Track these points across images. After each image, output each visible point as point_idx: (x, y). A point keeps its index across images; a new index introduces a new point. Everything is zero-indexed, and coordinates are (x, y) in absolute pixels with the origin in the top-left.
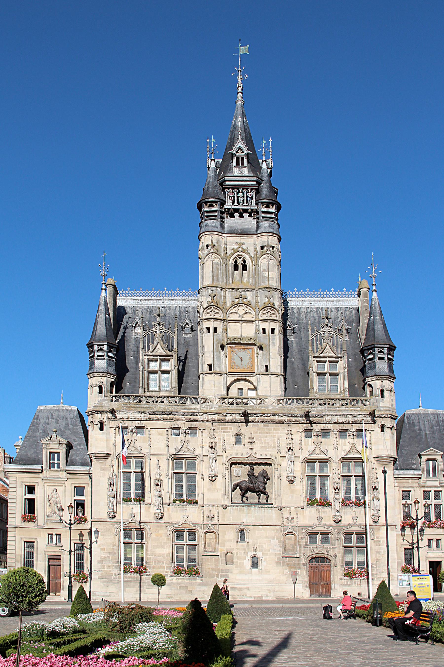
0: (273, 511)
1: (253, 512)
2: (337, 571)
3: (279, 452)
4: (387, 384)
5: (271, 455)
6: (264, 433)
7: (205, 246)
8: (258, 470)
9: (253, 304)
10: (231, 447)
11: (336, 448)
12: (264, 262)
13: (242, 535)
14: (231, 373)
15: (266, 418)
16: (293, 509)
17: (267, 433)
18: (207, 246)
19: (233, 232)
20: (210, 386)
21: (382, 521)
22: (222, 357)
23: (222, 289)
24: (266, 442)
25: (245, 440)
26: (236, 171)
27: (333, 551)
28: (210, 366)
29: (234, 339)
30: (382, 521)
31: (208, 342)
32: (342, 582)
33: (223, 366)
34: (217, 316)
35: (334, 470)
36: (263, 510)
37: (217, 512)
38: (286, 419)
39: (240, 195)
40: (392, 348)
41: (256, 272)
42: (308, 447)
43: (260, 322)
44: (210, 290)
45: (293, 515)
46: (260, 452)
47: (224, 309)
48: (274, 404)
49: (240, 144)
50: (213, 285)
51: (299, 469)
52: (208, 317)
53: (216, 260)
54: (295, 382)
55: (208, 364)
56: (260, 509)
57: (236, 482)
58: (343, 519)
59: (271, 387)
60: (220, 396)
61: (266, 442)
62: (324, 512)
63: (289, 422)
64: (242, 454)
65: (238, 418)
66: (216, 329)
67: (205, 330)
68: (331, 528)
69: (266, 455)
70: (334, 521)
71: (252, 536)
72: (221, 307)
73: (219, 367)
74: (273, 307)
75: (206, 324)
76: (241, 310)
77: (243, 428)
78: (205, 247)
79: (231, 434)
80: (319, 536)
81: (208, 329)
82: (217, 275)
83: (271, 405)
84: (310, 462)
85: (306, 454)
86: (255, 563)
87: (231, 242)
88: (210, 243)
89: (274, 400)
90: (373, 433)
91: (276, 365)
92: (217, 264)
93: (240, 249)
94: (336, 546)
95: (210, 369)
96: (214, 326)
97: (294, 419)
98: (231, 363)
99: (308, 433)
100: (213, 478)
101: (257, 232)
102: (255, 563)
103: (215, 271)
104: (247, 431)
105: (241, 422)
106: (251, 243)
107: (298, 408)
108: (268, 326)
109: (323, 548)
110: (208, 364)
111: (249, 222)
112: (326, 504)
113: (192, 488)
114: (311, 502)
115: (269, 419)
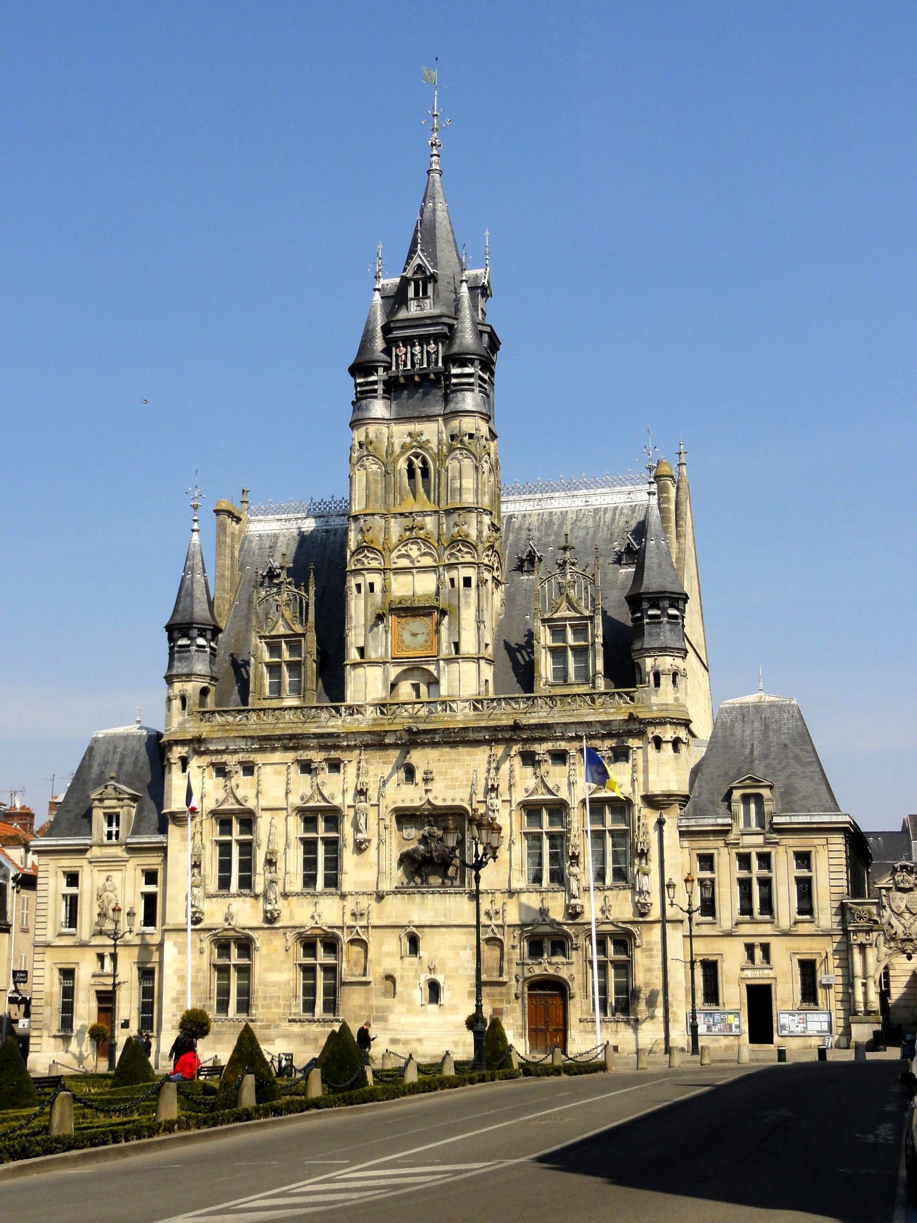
2: (575, 1007)
3: (473, 793)
5: (462, 800)
6: (450, 760)
7: (357, 445)
9: (434, 541)
10: (395, 790)
11: (572, 783)
14: (397, 661)
16: (498, 895)
17: (456, 760)
18: (361, 445)
21: (655, 913)
23: (383, 516)
25: (419, 776)
26: (413, 305)
27: (568, 969)
28: (362, 651)
29: (400, 603)
30: (655, 913)
31: (358, 609)
32: (585, 1028)
33: (381, 651)
34: (374, 564)
39: (418, 348)
44: (362, 521)
46: (446, 793)
47: (383, 552)
48: (467, 710)
50: (368, 511)
53: (375, 467)
55: (357, 648)
57: (405, 850)
58: (586, 909)
60: (377, 702)
61: (452, 780)
62: (552, 898)
64: (412, 801)
65: (406, 737)
66: (372, 585)
67: (354, 590)
69: (453, 800)
72: (380, 548)
73: (376, 651)
74: (466, 543)
76: (414, 551)
78: (357, 447)
80: (547, 945)
81: (358, 586)
82: (376, 492)
83: (463, 715)
85: (519, 796)
86: (434, 990)
87: (400, 433)
88: (363, 439)
89: (467, 704)
92: (375, 473)
93: (417, 444)
94: (574, 959)
95: (362, 656)
96: (368, 581)
102: (434, 990)
103: (373, 488)
109: (550, 963)
110: (357, 648)
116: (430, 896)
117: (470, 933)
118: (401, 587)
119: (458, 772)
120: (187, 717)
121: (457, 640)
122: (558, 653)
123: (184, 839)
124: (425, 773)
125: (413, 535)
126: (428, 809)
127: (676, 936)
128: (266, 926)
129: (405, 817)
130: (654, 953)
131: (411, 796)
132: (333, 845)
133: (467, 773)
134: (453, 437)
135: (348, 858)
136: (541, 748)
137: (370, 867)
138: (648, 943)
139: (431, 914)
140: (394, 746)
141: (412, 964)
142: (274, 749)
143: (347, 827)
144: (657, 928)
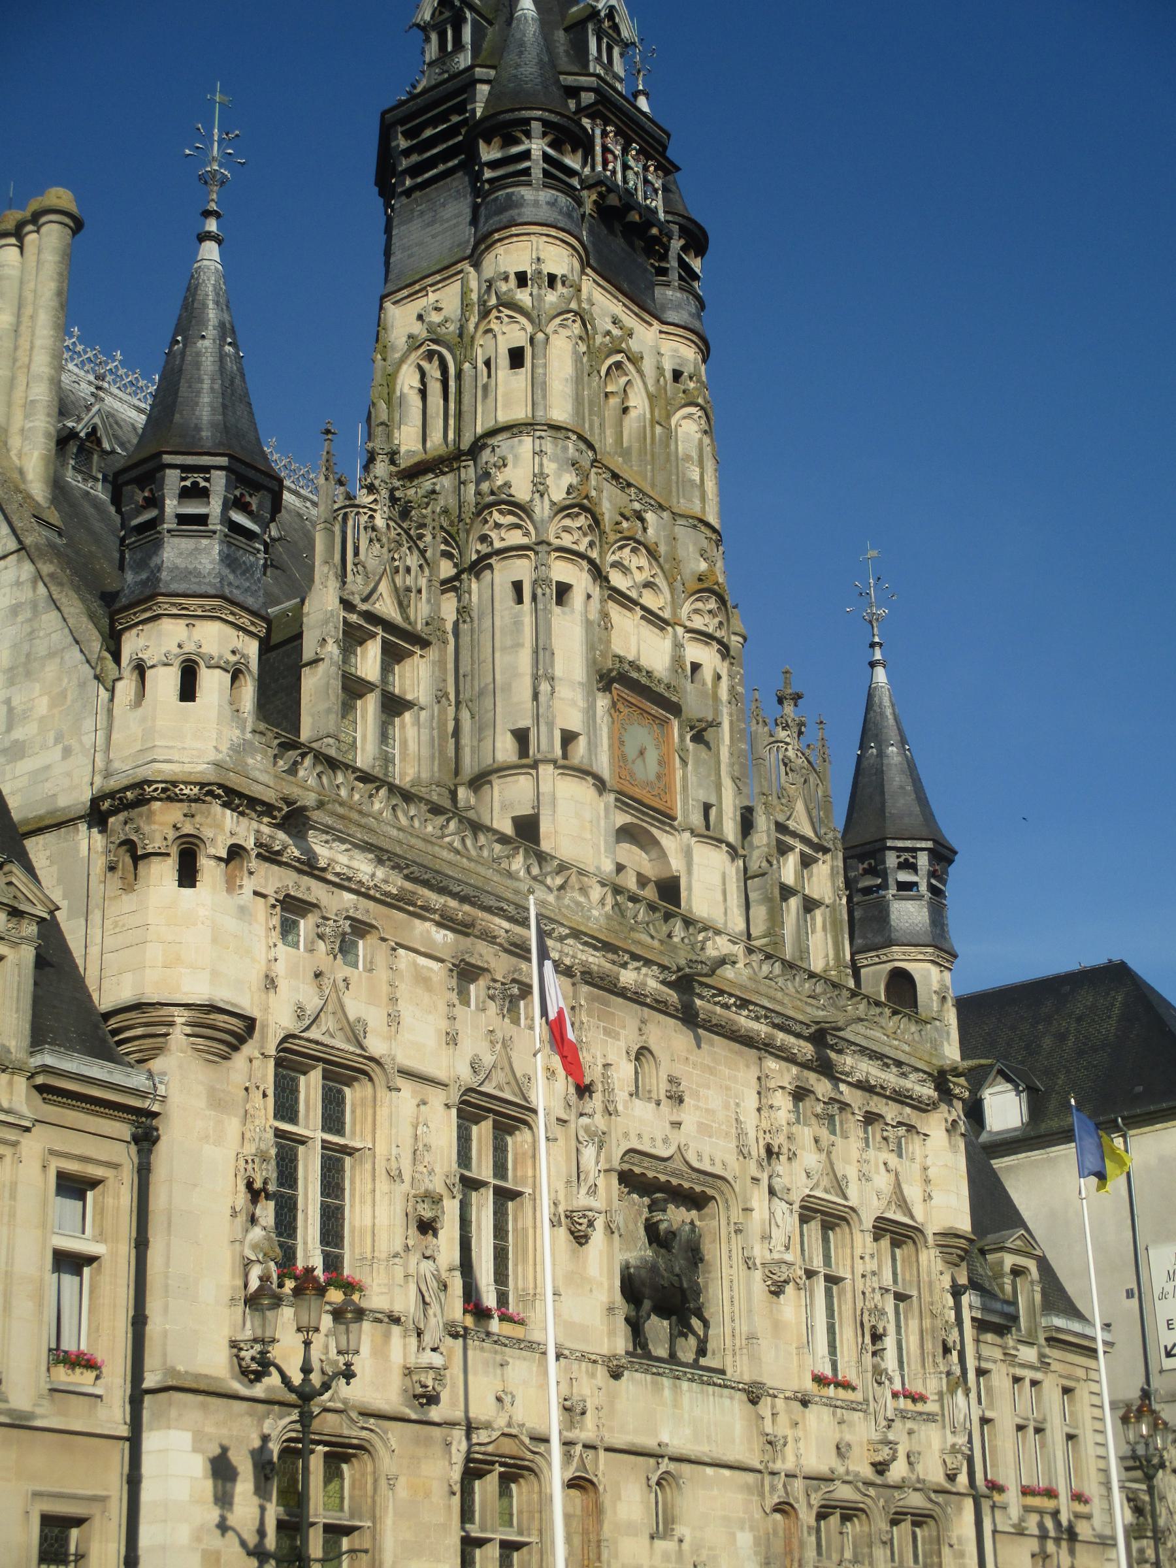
0: (736, 1404)
1: (686, 1399)
15: (718, 1009)
16: (780, 1403)
22: (599, 721)
36: (711, 1398)
37: (591, 1386)
38: (761, 1029)
43: (688, 635)
45: (782, 1429)
52: (567, 541)
56: (702, 1392)
63: (765, 1047)
65: (652, 983)
68: (872, 1492)
70: (873, 1464)
75: (561, 571)
79: (622, 1044)
97: (781, 1037)
105: (660, 1007)
116: (685, 1385)
117: (748, 1488)
120: (249, 736)
121: (713, 800)
123: (217, 1102)
124: (672, 1080)
126: (673, 1174)
128: (414, 1416)
130: (967, 1561)
133: (726, 1106)
134: (677, 375)
138: (959, 1539)
139: (688, 1431)
140: (635, 997)
141: (666, 1557)
142: (423, 912)
144: (969, 1504)
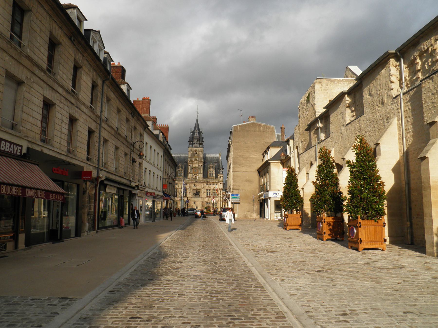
4: (222, 175)
8: (198, 191)
11: (212, 187)
12: (200, 153)
13: (195, 203)
19: (195, 147)
20: (190, 176)
24: (200, 186)
31: (190, 168)
35: (211, 191)
40: (223, 169)
41: (199, 155)
42: (207, 187)
47: (193, 162)
49: (197, 130)
51: (205, 190)
54: (205, 175)
59: (200, 176)
61: (200, 186)
71: (197, 203)
77: (196, 184)
84: (207, 190)
87: (194, 149)
90: (219, 184)
91: (202, 172)
98: (194, 172)
99: (207, 184)
100: (190, 193)
101: (199, 147)
104: (196, 184)
106: (198, 149)
107: (205, 180)
108: (200, 165)
111: (198, 145)
112: (210, 197)
113: (186, 194)
114: (207, 197)
115: (200, 182)
118: (194, 166)
119: (200, 185)
122: (210, 174)
125: (196, 160)
127: (222, 202)
129: (194, 190)
131: (195, 188)
132: (186, 192)
135: (188, 194)
136: (209, 183)
137: (190, 195)
143: (188, 191)
